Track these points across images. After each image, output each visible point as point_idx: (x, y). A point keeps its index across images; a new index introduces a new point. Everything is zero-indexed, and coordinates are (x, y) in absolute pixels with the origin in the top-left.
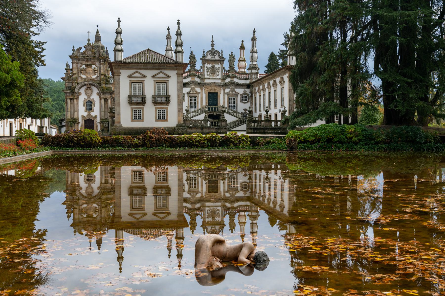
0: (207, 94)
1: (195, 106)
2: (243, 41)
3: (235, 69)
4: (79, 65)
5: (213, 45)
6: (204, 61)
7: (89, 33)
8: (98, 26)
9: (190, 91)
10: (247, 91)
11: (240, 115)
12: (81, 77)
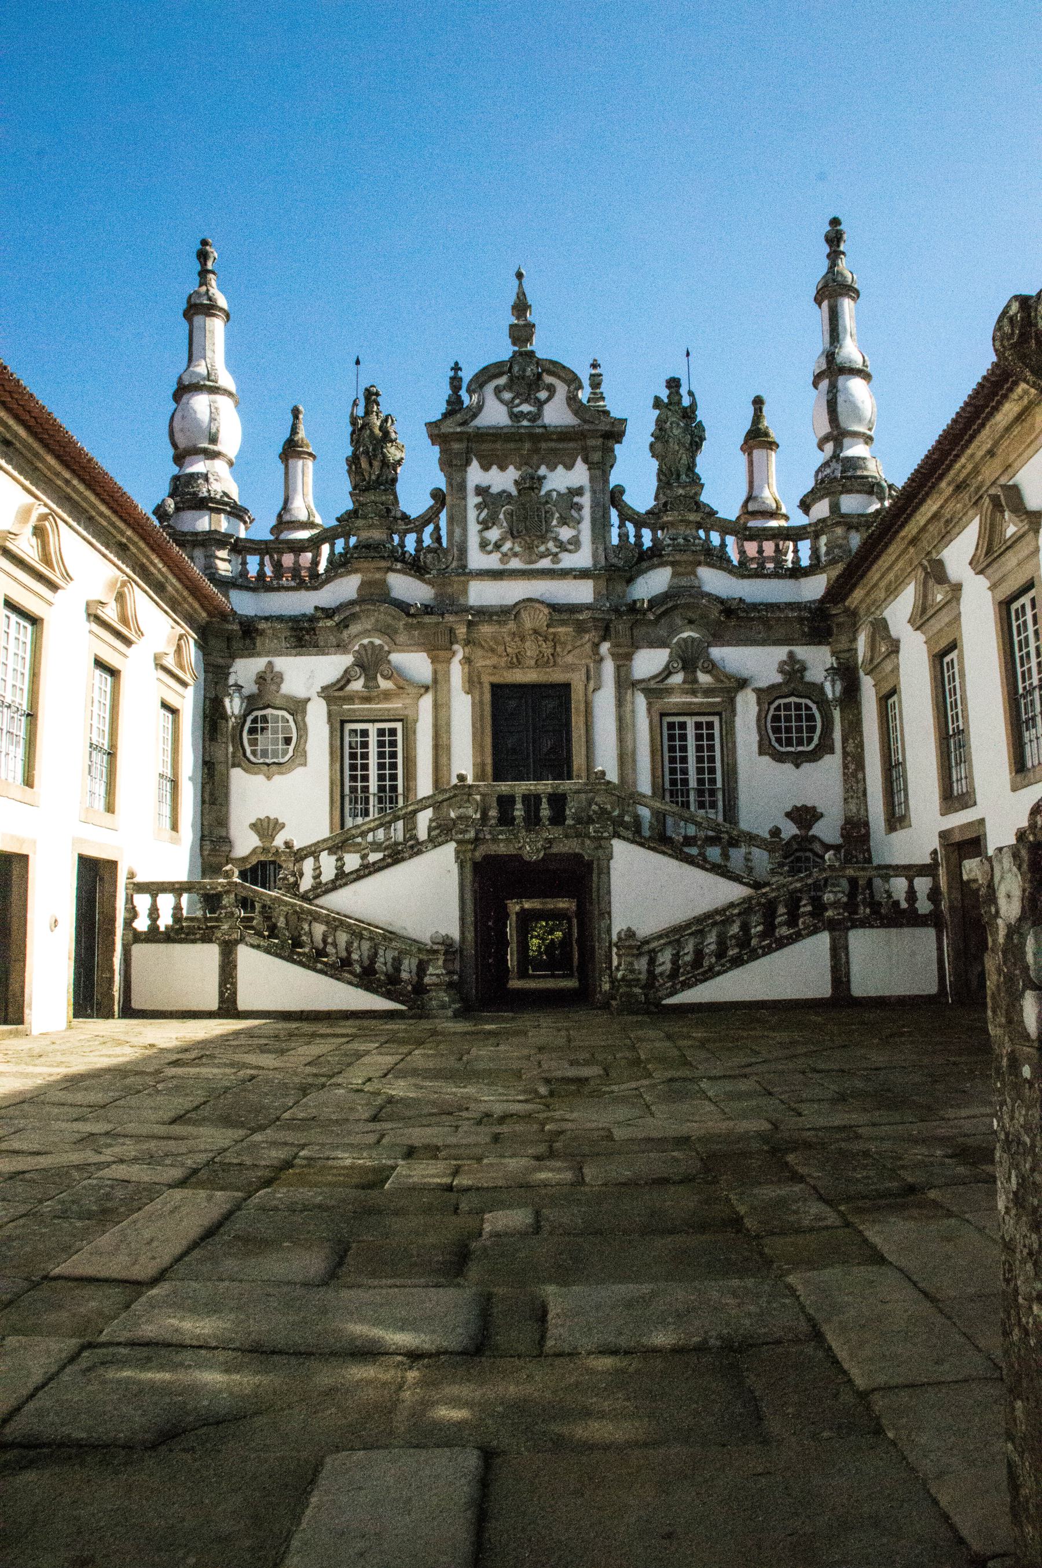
0: (487, 697)
1: (388, 793)
2: (758, 402)
3: (704, 498)
5: (521, 333)
6: (456, 446)
9: (346, 678)
10: (809, 665)
11: (761, 858)
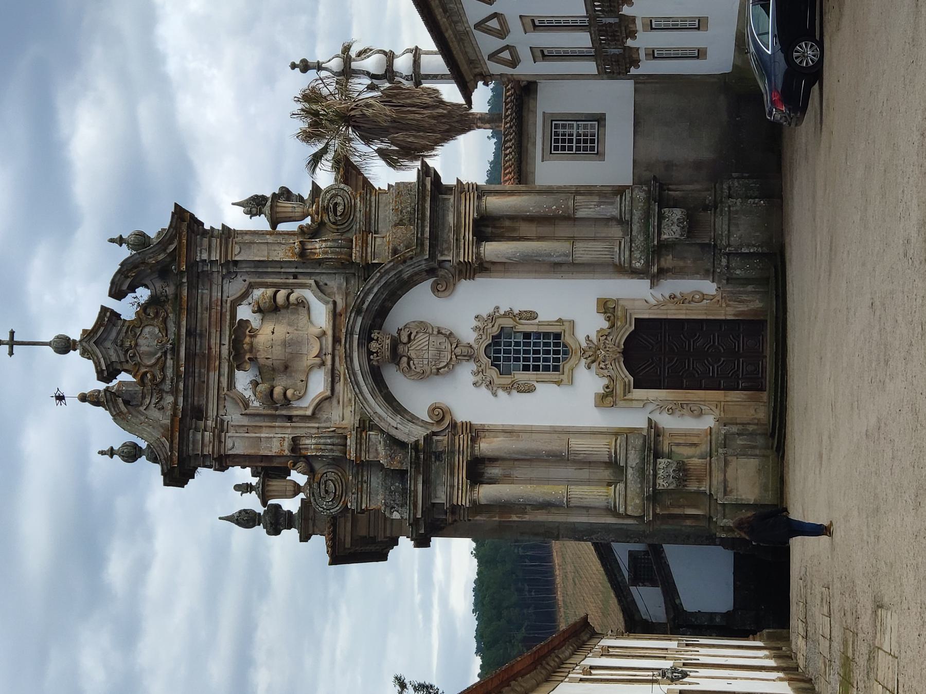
4: (234, 416)
7: (12, 343)
8: (60, 398)
12: (318, 407)
